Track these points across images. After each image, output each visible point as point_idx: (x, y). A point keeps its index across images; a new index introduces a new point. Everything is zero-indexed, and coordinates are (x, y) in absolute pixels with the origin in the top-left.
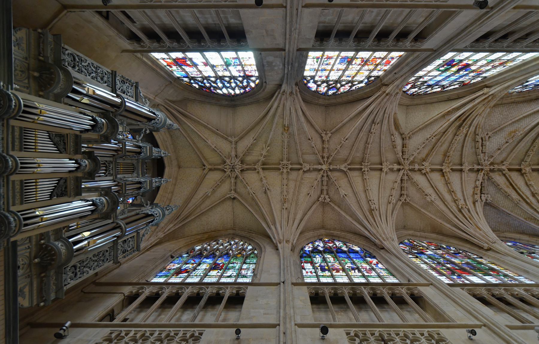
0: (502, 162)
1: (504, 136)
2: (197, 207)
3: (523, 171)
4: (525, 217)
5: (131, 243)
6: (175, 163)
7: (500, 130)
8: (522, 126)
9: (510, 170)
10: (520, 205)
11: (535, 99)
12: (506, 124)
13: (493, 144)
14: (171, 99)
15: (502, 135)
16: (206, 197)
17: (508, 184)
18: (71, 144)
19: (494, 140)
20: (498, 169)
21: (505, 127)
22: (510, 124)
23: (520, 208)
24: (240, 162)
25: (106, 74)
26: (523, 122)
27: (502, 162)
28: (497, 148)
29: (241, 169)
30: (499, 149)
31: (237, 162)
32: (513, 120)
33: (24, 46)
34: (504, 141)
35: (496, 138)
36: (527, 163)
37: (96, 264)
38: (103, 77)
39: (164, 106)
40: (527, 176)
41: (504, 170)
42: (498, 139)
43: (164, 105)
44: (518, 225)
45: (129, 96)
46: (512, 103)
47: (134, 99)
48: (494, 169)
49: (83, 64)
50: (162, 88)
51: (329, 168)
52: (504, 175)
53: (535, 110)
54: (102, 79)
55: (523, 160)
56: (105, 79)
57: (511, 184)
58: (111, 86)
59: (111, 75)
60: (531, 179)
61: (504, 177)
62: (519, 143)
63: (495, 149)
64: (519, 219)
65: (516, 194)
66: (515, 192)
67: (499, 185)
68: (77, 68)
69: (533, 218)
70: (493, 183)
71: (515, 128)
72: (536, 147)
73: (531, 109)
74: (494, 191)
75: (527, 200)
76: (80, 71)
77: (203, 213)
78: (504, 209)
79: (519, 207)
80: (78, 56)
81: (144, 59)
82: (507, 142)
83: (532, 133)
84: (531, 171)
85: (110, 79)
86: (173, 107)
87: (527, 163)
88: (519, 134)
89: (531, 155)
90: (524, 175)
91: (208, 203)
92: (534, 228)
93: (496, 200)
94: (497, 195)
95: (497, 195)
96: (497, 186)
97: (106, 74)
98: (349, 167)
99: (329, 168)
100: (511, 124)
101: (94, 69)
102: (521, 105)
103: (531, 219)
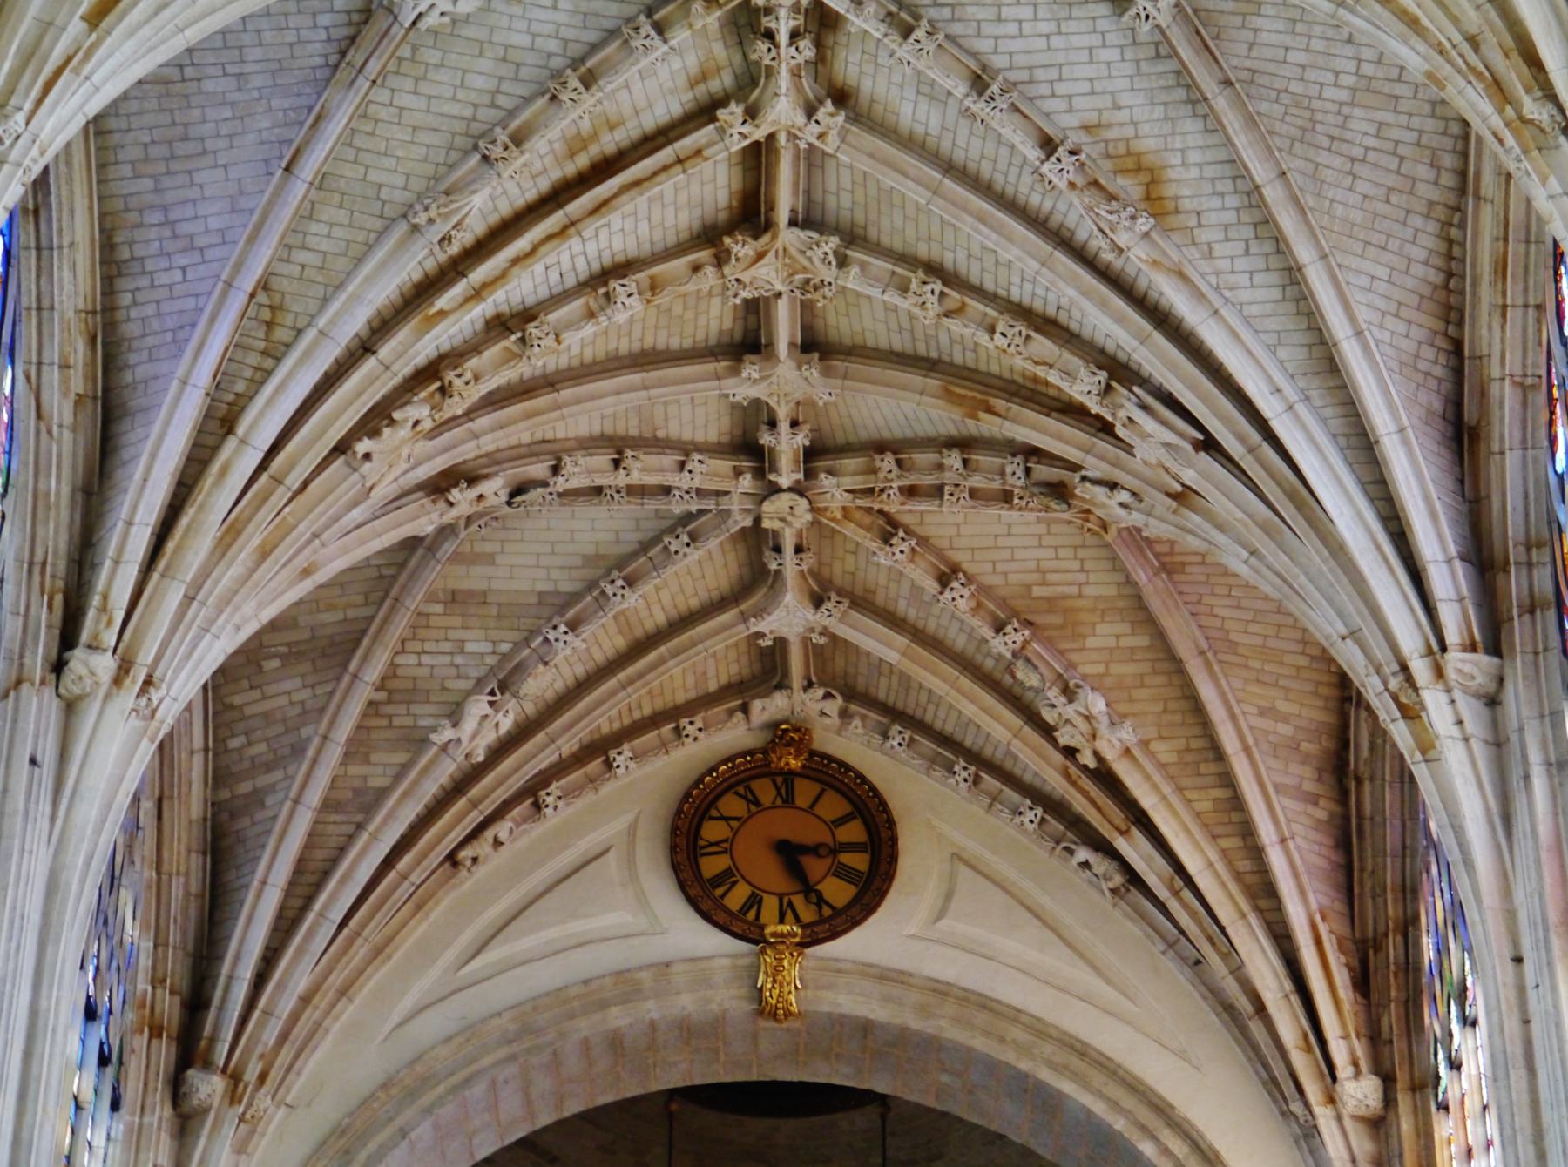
0: (841, 97)
1: (1123, 116)
3: (741, 247)
4: (275, 283)
7: (1191, 86)
8: (1209, 255)
9: (758, 158)
10: (402, 245)
11: (1457, 348)
12: (1241, 141)
13: (1044, 27)
15: (1125, 99)
17: (609, 143)
19: (1086, 41)
20: (770, 72)
21: (1213, 125)
22: (1234, 161)
23: (370, 247)
26: (1241, 264)
27: (841, 97)
28: (999, 62)
30: (979, 83)
32: (1273, 194)
34: (1065, 123)
35: (1112, 55)
36: (829, 274)
40: (696, 268)
41: (752, 113)
42: (1090, 71)
44: (184, 228)
46: (1462, 174)
48: (770, 36)
52: (705, 113)
53: (1350, 352)
55: (853, 238)
57: (604, 168)
60: (662, 299)
61: (677, 110)
62: (1037, 223)
63: (984, 46)
64: (252, 240)
65: (505, 209)
66: (531, 195)
67: (588, 81)
69: (281, 334)
70: (612, 34)
71: (1186, 204)
72: (983, 337)
73: (1363, 314)
74: (525, 40)
75: (458, 290)
78: (334, 128)
79: (382, 234)
82: (1048, 145)
83: (1120, 320)
84: (745, 294)
87: (829, 274)
88: (1122, 239)
89: (905, 304)
90: (704, 255)
92: (179, 346)
93: (433, 56)
94: (485, 65)
95: (485, 65)
96: (576, 63)
100: (1237, 170)
102: (1424, 243)
103: (270, 325)
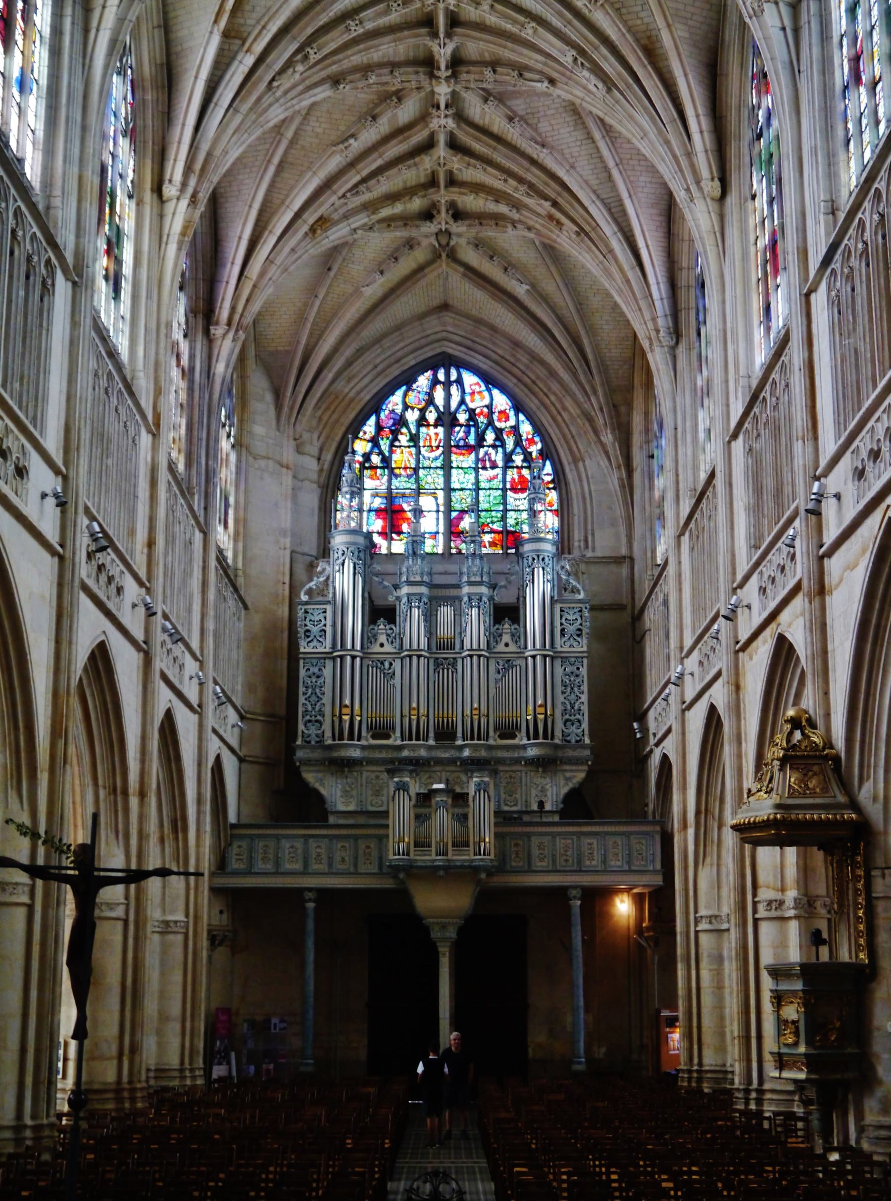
2: (561, 319)
5: (570, 617)
6: (433, 325)
14: (272, 412)
16: (535, 289)
18: (422, 810)
24: (428, 224)
25: (309, 669)
29: (451, 221)
31: (430, 228)
33: (320, 775)
37: (576, 689)
38: (314, 674)
39: (294, 425)
43: (292, 426)
45: (325, 618)
47: (329, 608)
49: (310, 708)
50: (262, 463)
51: (447, 79)
54: (318, 677)
56: (315, 670)
58: (322, 661)
59: (307, 660)
68: (319, 718)
76: (321, 713)
77: (578, 310)
80: (303, 717)
81: (240, 565)
85: (314, 661)
86: (291, 397)
91: (551, 286)
97: (309, 669)
98: (442, 35)
99: (447, 77)
101: (310, 691)
